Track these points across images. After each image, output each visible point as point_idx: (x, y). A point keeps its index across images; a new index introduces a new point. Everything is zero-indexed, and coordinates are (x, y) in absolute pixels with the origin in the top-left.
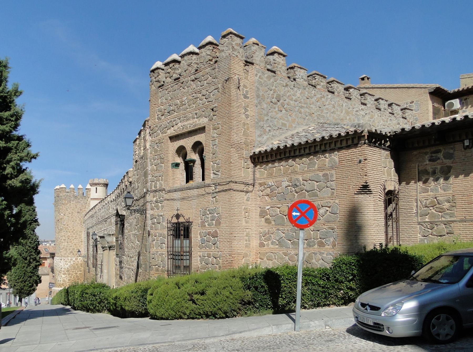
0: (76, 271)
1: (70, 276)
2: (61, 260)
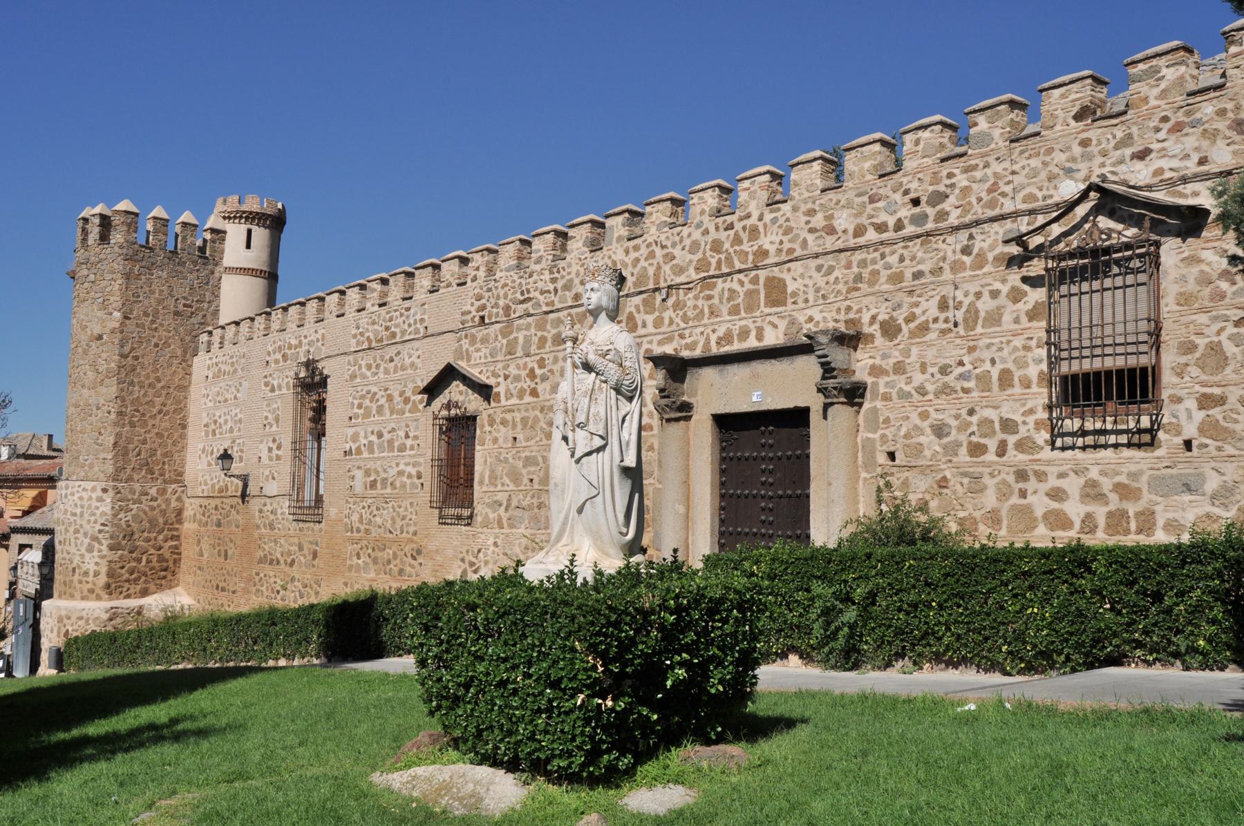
0: (161, 537)
2: (105, 490)
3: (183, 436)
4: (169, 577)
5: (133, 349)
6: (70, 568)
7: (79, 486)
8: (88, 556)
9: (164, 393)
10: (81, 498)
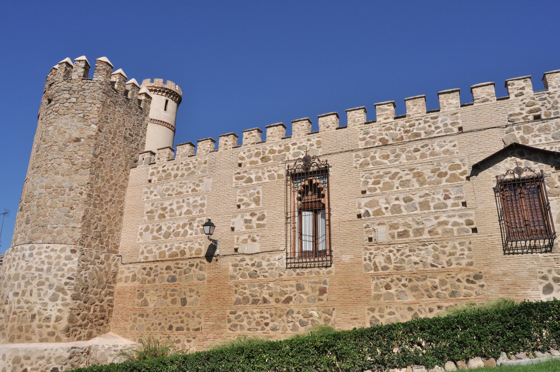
0: (103, 292)
1: (87, 305)
2: (73, 251)
3: (121, 221)
4: (105, 324)
5: (101, 153)
6: (29, 315)
7: (47, 248)
8: (50, 304)
9: (114, 188)
10: (49, 257)
